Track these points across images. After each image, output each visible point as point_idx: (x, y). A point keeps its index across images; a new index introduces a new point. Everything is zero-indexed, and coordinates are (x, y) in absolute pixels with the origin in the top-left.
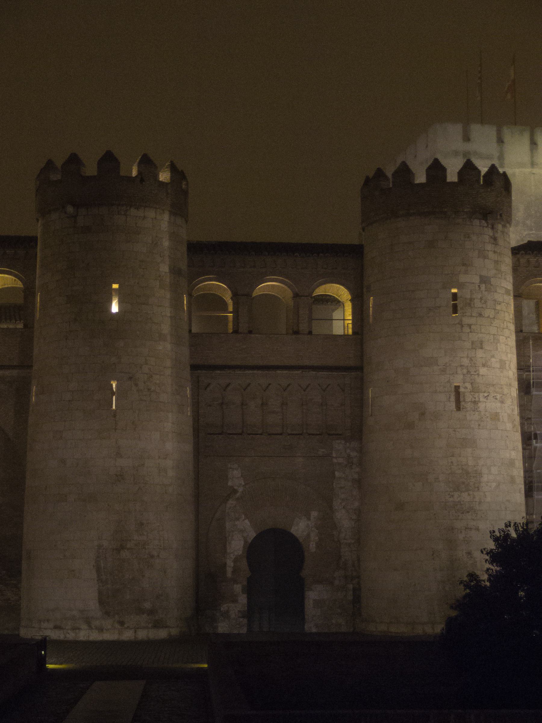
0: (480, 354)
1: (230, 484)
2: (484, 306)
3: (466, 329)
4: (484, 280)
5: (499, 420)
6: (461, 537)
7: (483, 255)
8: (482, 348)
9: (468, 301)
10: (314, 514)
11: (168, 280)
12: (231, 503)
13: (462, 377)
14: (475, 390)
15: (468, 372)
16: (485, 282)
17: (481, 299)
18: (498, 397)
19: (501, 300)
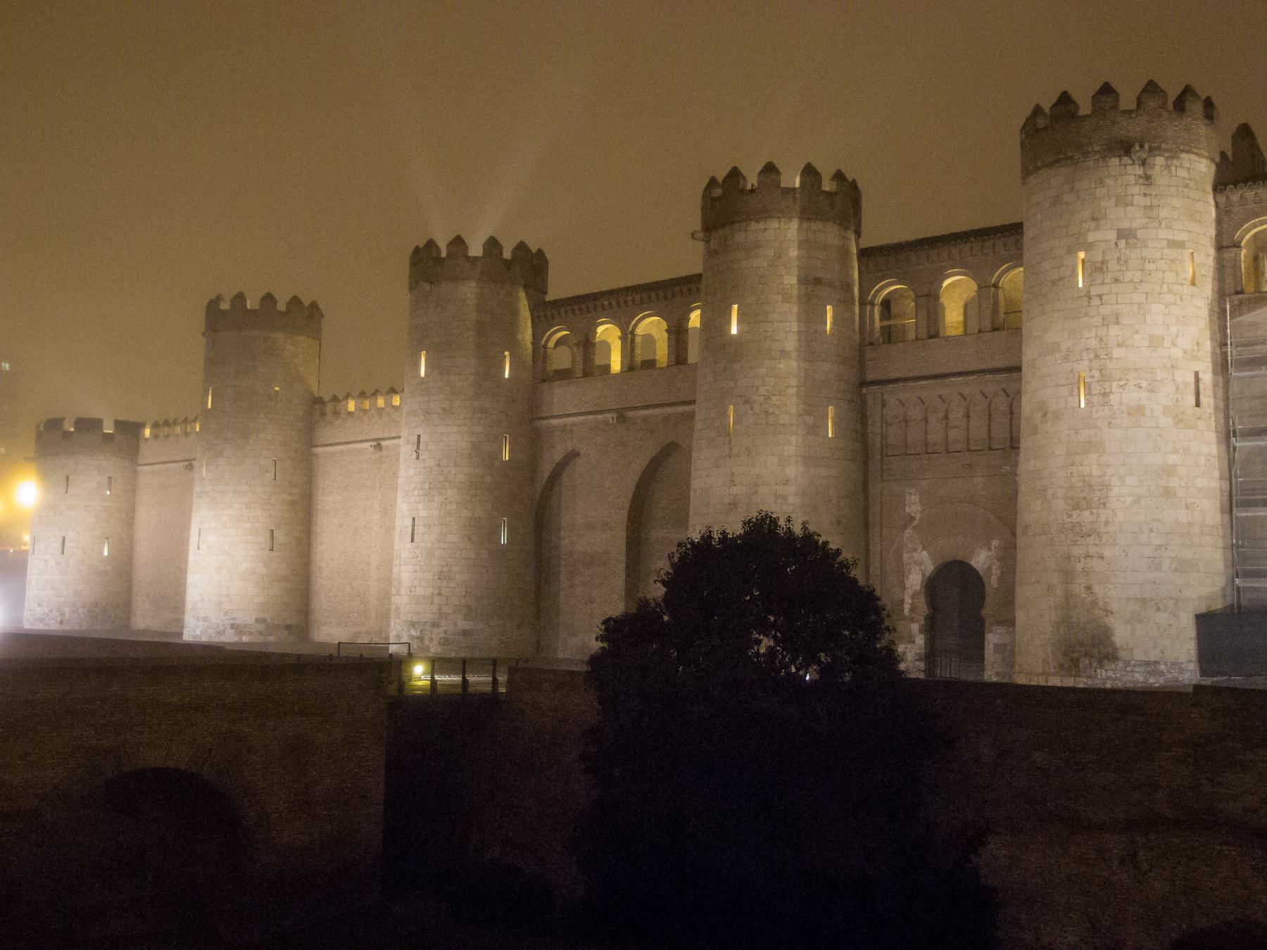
0: (1114, 331)
1: (907, 510)
2: (1124, 268)
3: (1096, 302)
4: (1123, 234)
5: (1143, 415)
6: (1079, 567)
7: (1123, 201)
8: (1117, 323)
9: (1099, 265)
10: (995, 543)
11: (796, 292)
12: (908, 532)
13: (1087, 363)
14: (1105, 378)
15: (1097, 356)
16: (1126, 237)
17: (1119, 259)
18: (1144, 384)
19: (1158, 255)
